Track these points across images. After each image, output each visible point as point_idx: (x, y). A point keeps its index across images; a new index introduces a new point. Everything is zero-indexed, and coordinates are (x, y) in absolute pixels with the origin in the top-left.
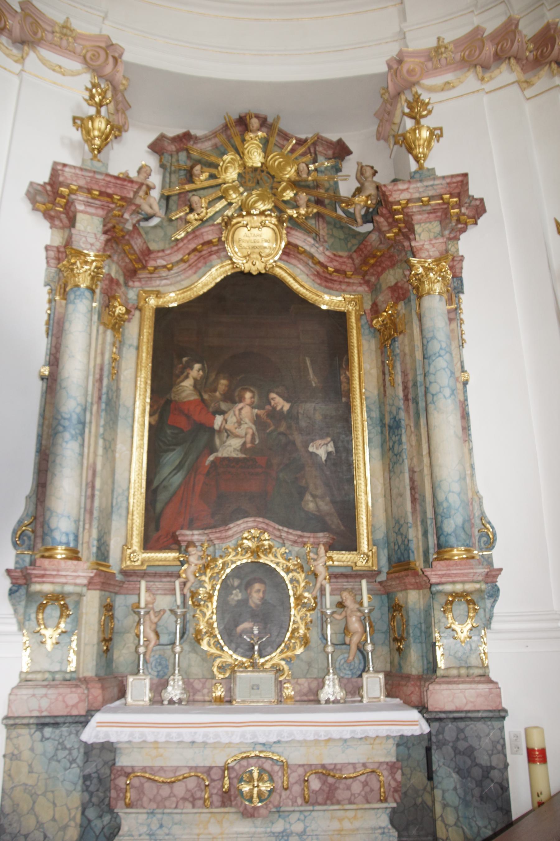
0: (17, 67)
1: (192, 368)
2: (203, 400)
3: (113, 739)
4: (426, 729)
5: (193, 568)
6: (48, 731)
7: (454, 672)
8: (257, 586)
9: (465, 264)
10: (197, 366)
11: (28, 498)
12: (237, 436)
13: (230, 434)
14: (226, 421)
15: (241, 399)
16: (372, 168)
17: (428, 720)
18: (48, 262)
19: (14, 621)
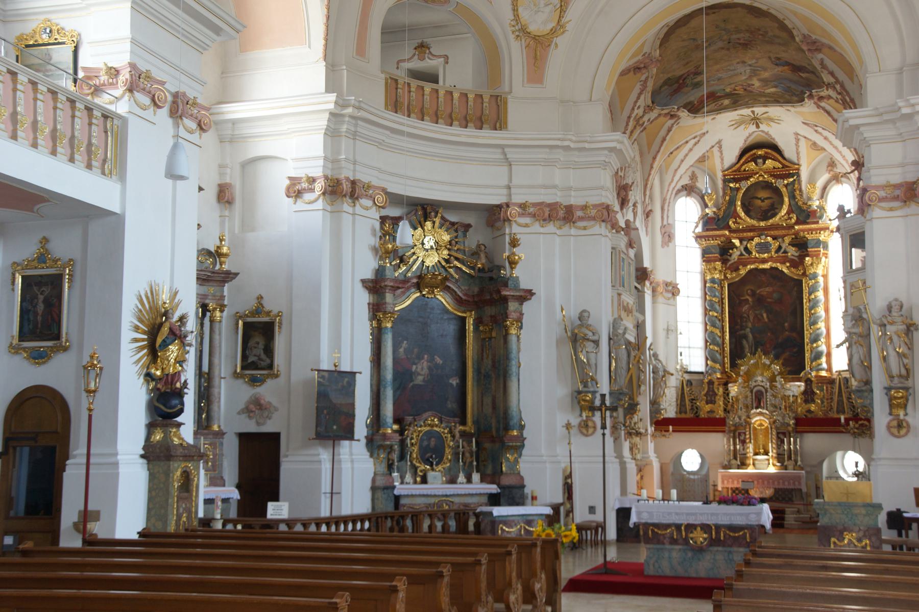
0: (350, 210)
1: (403, 343)
2: (407, 357)
3: (402, 494)
4: (499, 491)
5: (411, 432)
6: (385, 491)
7: (509, 472)
8: (433, 439)
9: (524, 316)
10: (405, 342)
11: (369, 409)
12: (422, 375)
13: (419, 374)
14: (417, 368)
15: (423, 358)
16: (484, 245)
17: (500, 488)
18: (369, 310)
19: (368, 454)
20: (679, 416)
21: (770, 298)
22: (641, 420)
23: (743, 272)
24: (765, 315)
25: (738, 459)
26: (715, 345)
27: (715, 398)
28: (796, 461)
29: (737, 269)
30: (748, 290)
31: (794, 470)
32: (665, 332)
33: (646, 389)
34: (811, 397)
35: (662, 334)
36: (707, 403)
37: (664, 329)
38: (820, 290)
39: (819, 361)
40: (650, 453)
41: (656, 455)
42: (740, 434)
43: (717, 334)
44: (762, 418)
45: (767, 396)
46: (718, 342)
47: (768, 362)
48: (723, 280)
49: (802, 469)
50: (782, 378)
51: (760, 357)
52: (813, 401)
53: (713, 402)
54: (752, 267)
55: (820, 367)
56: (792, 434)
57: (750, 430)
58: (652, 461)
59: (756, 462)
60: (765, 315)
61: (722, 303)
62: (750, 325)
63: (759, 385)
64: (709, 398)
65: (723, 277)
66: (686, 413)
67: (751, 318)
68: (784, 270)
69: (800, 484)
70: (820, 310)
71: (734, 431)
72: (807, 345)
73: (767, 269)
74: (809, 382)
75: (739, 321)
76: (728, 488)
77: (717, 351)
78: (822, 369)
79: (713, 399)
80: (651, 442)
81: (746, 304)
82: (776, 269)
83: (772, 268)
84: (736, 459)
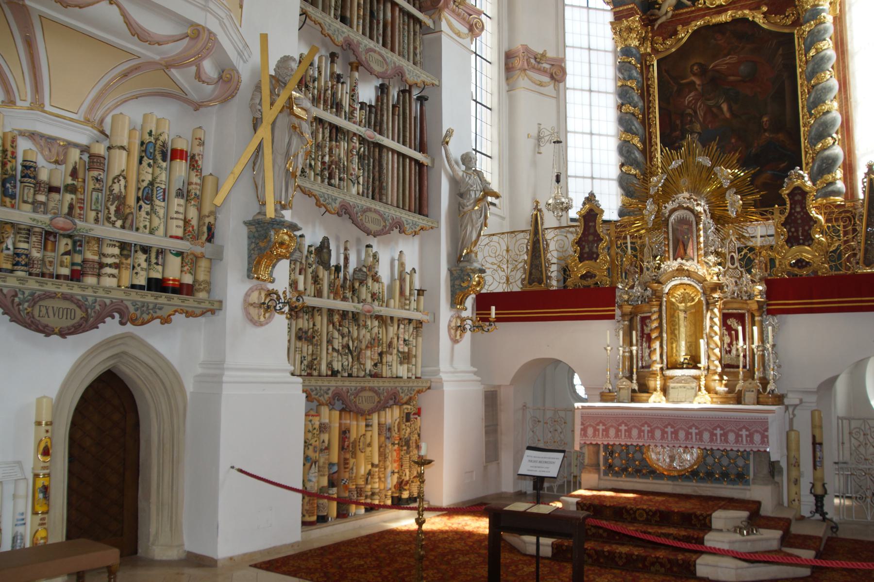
20: (528, 288)
21: (733, 75)
22: (421, 292)
23: (684, 34)
24: (725, 107)
25: (635, 376)
26: (631, 165)
27: (597, 247)
28: (764, 382)
29: (675, 33)
30: (693, 65)
31: (758, 403)
32: (532, 142)
33: (438, 227)
34: (804, 230)
35: (526, 147)
36: (581, 259)
37: (528, 136)
38: (828, 39)
39: (829, 178)
40: (444, 365)
41: (475, 369)
42: (643, 320)
43: (636, 146)
44: (686, 280)
45: (698, 230)
46: (635, 160)
47: (707, 162)
48: (650, 55)
49: (779, 399)
50: (736, 193)
51: (690, 152)
52: (808, 239)
53: (592, 256)
54: (700, 23)
55: (831, 188)
56: (757, 319)
57: (660, 311)
58: (440, 382)
59: (671, 384)
60: (725, 107)
61: (649, 95)
62: (698, 127)
63: (681, 207)
64: (587, 250)
65: (649, 50)
66: (540, 281)
67: (700, 114)
68: (757, 20)
69: (765, 439)
70: (828, 77)
71: (631, 317)
72: (806, 153)
73: (726, 23)
74: (798, 198)
75: (678, 122)
76: (597, 445)
77: (635, 175)
78: (837, 193)
79: (595, 250)
80: (455, 341)
81: (690, 92)
82: (744, 20)
83: (735, 21)
84: (630, 378)
